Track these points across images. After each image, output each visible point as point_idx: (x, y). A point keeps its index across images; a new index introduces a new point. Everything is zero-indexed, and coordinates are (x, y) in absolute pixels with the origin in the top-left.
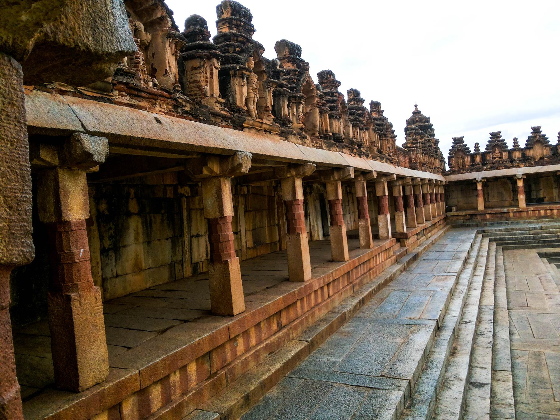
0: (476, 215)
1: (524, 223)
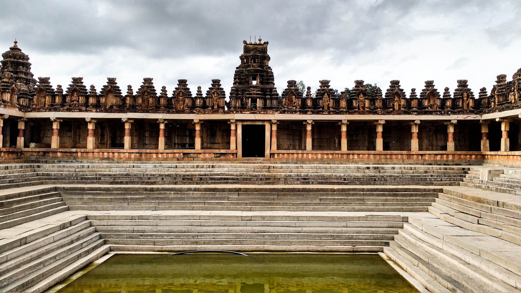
0: (48, 152)
1: (87, 162)
